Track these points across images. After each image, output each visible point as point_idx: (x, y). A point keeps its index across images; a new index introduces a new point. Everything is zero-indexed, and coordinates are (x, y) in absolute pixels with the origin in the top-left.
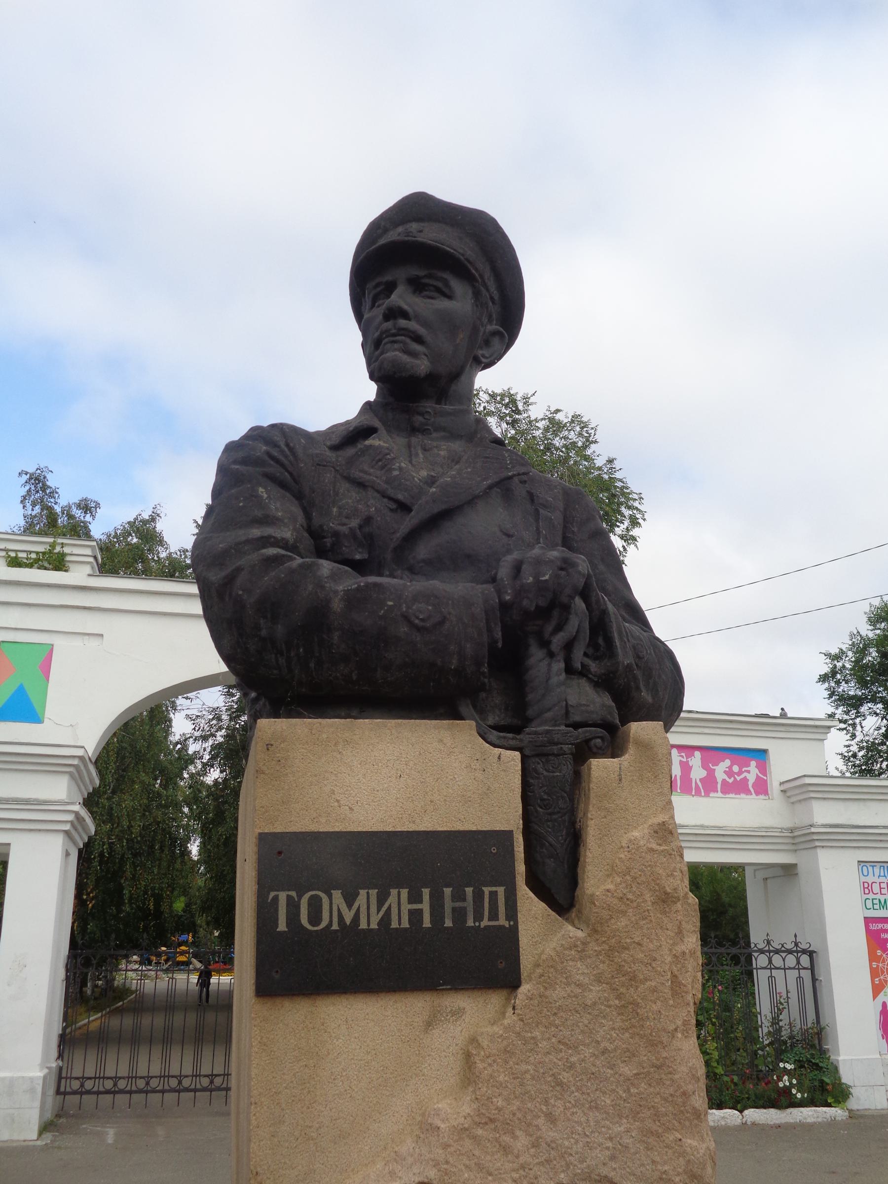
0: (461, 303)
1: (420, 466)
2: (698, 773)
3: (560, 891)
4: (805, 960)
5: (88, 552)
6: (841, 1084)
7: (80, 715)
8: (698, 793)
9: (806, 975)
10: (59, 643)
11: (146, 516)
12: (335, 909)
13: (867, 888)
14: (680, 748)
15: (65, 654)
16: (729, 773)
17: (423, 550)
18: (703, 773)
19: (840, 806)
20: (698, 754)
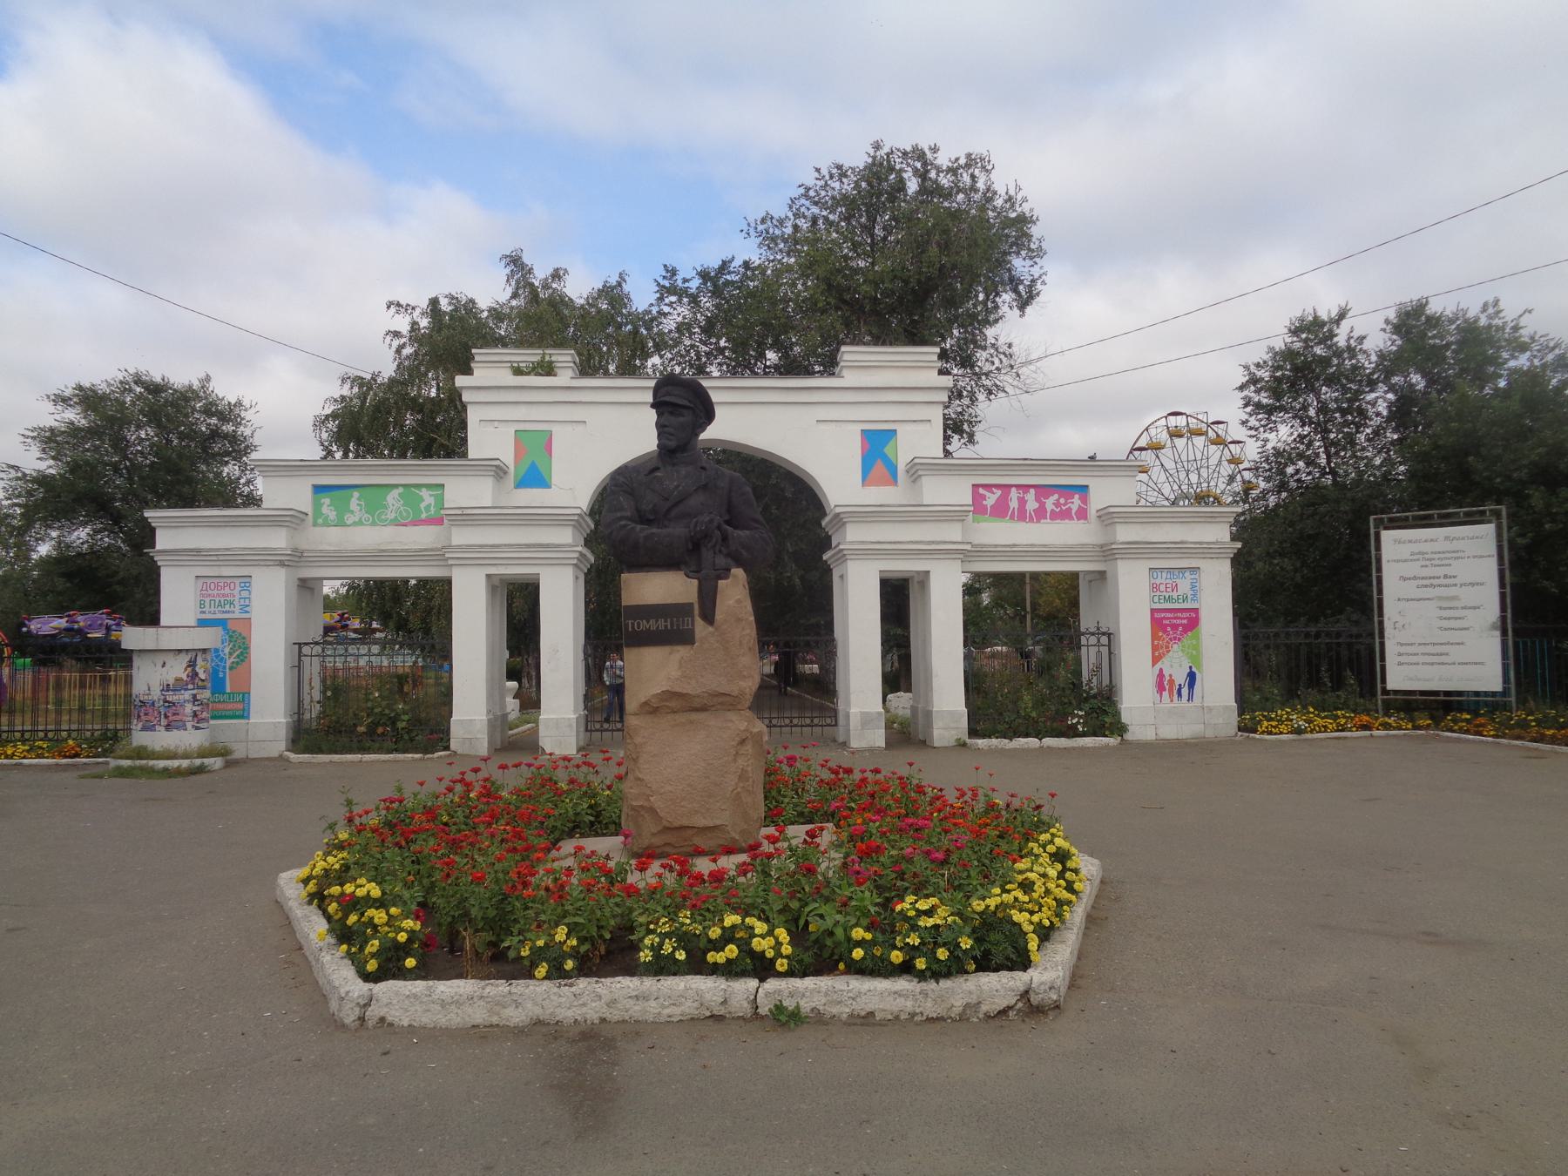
0: (687, 418)
1: (676, 479)
2: (1032, 505)
3: (709, 618)
4: (1104, 640)
5: (569, 358)
6: (1119, 722)
7: (577, 479)
8: (1031, 520)
9: (1105, 650)
10: (555, 429)
11: (613, 281)
12: (644, 625)
13: (1155, 588)
14: (1018, 487)
15: (562, 439)
16: (1057, 504)
17: (673, 513)
18: (1036, 505)
19: (1138, 527)
20: (1032, 491)
